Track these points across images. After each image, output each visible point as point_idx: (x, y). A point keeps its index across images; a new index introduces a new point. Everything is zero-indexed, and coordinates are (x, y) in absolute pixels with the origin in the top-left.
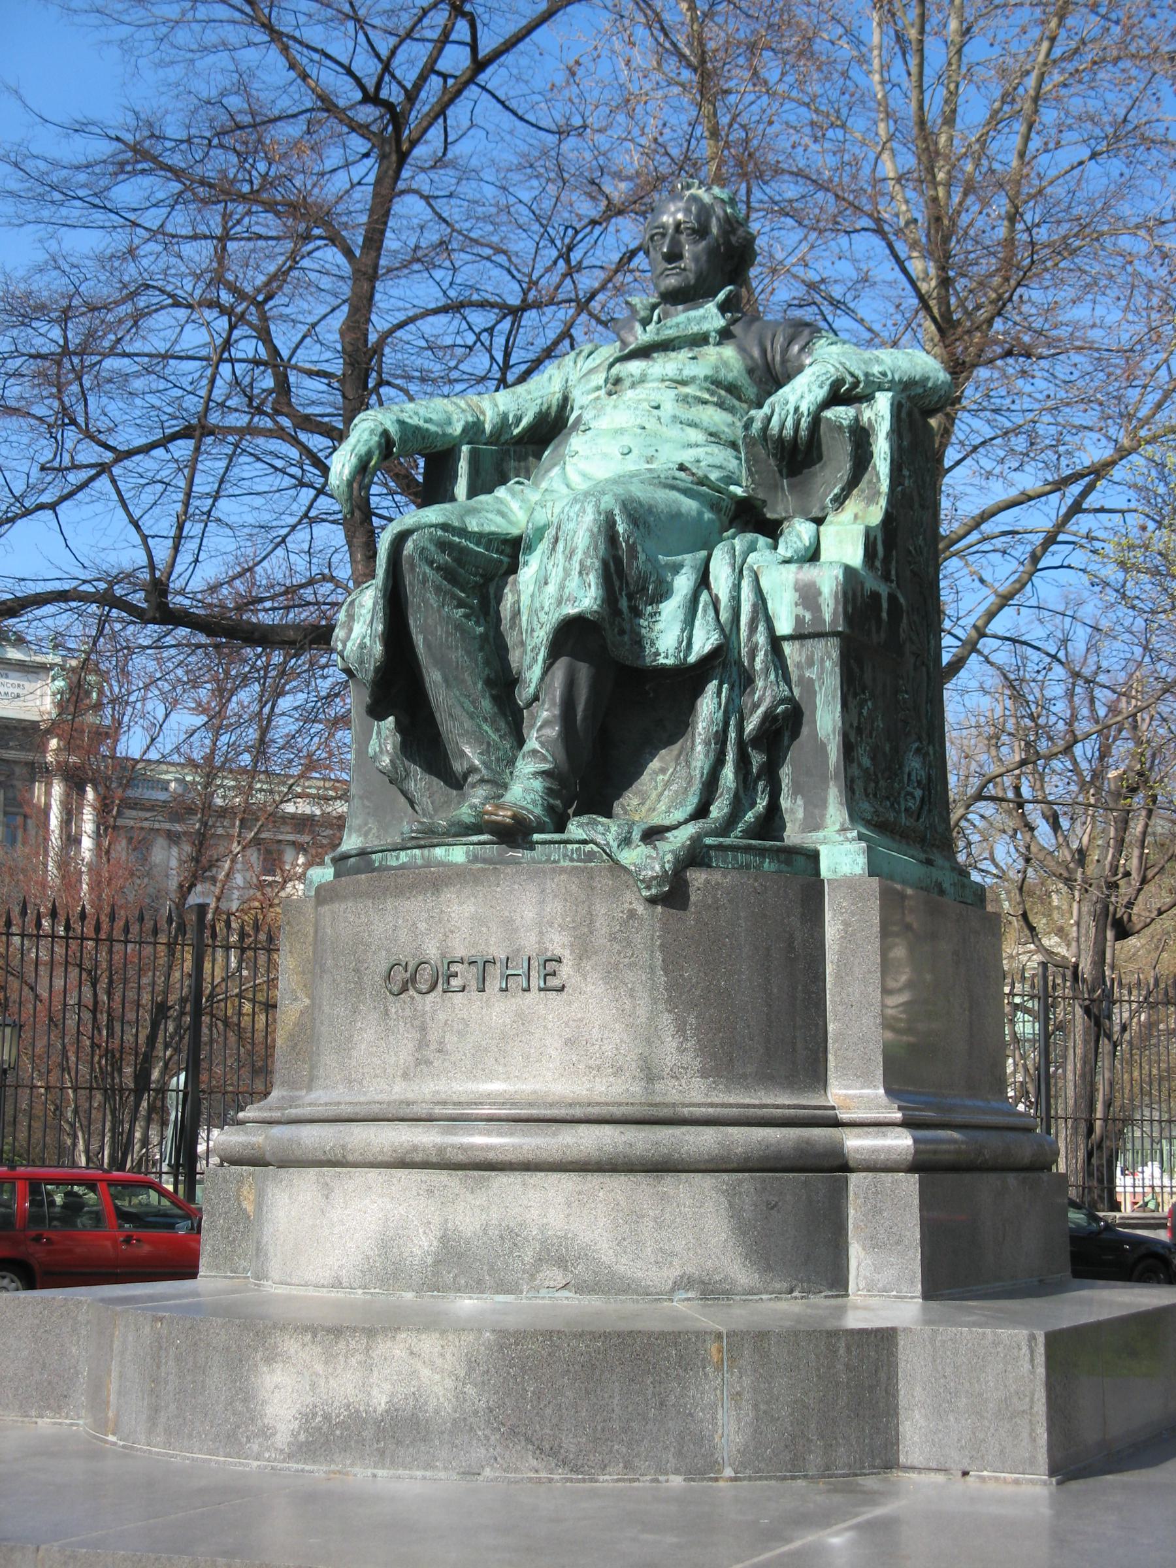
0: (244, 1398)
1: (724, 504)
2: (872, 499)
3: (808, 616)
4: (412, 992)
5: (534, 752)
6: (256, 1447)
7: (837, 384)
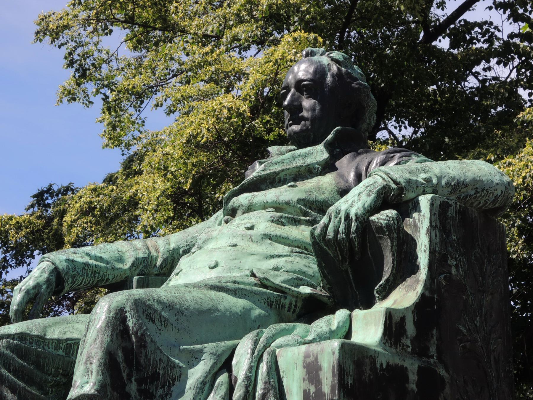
1: (287, 302)
2: (411, 288)
3: (312, 389)
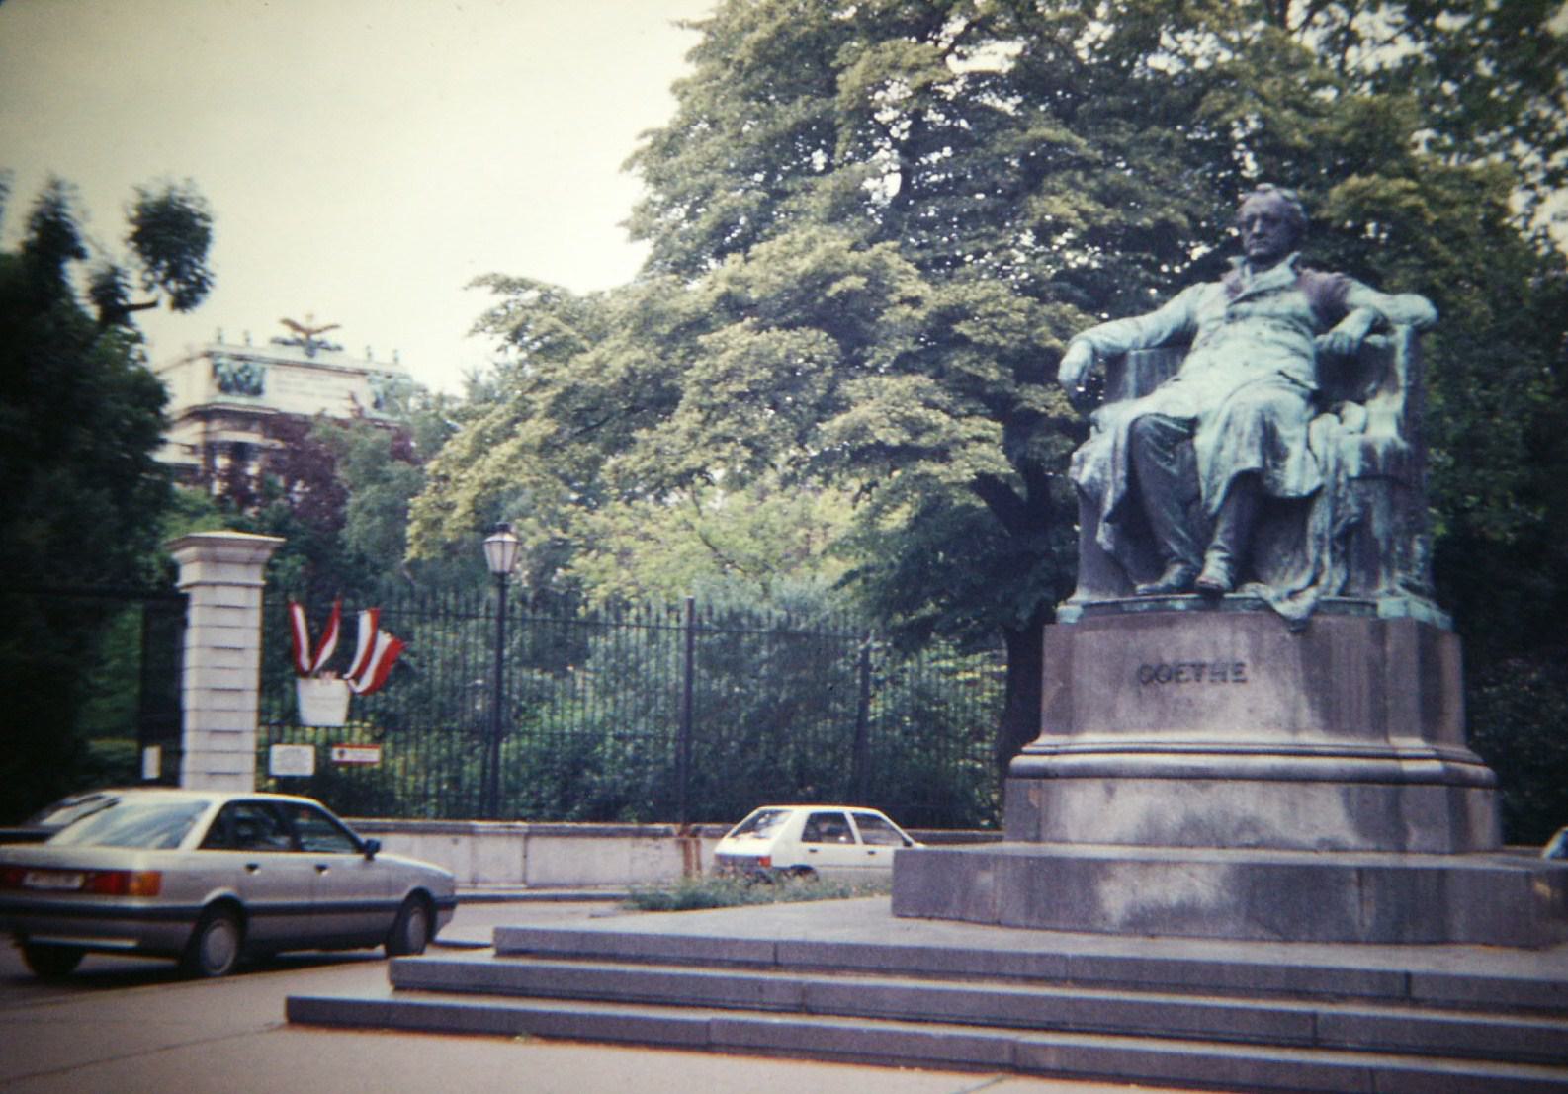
0: (1092, 900)
7: (1375, 321)
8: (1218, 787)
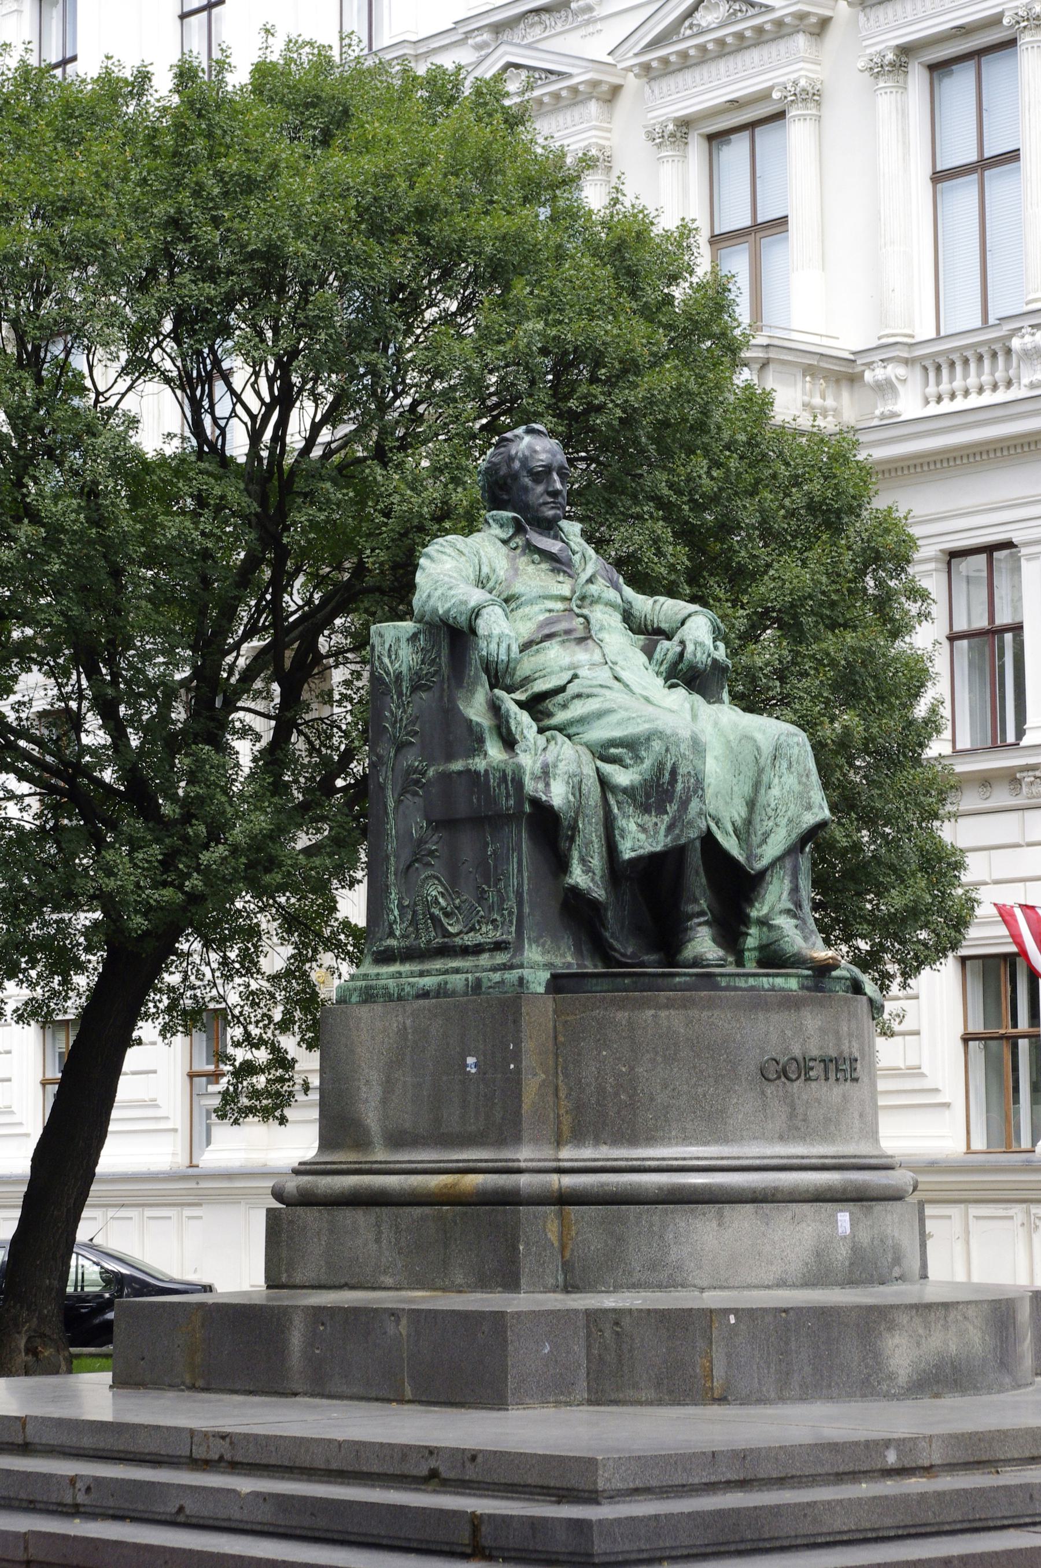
0: (874, 1356)
4: (783, 1079)
5: (788, 911)
6: (885, 1388)
8: (879, 1207)
